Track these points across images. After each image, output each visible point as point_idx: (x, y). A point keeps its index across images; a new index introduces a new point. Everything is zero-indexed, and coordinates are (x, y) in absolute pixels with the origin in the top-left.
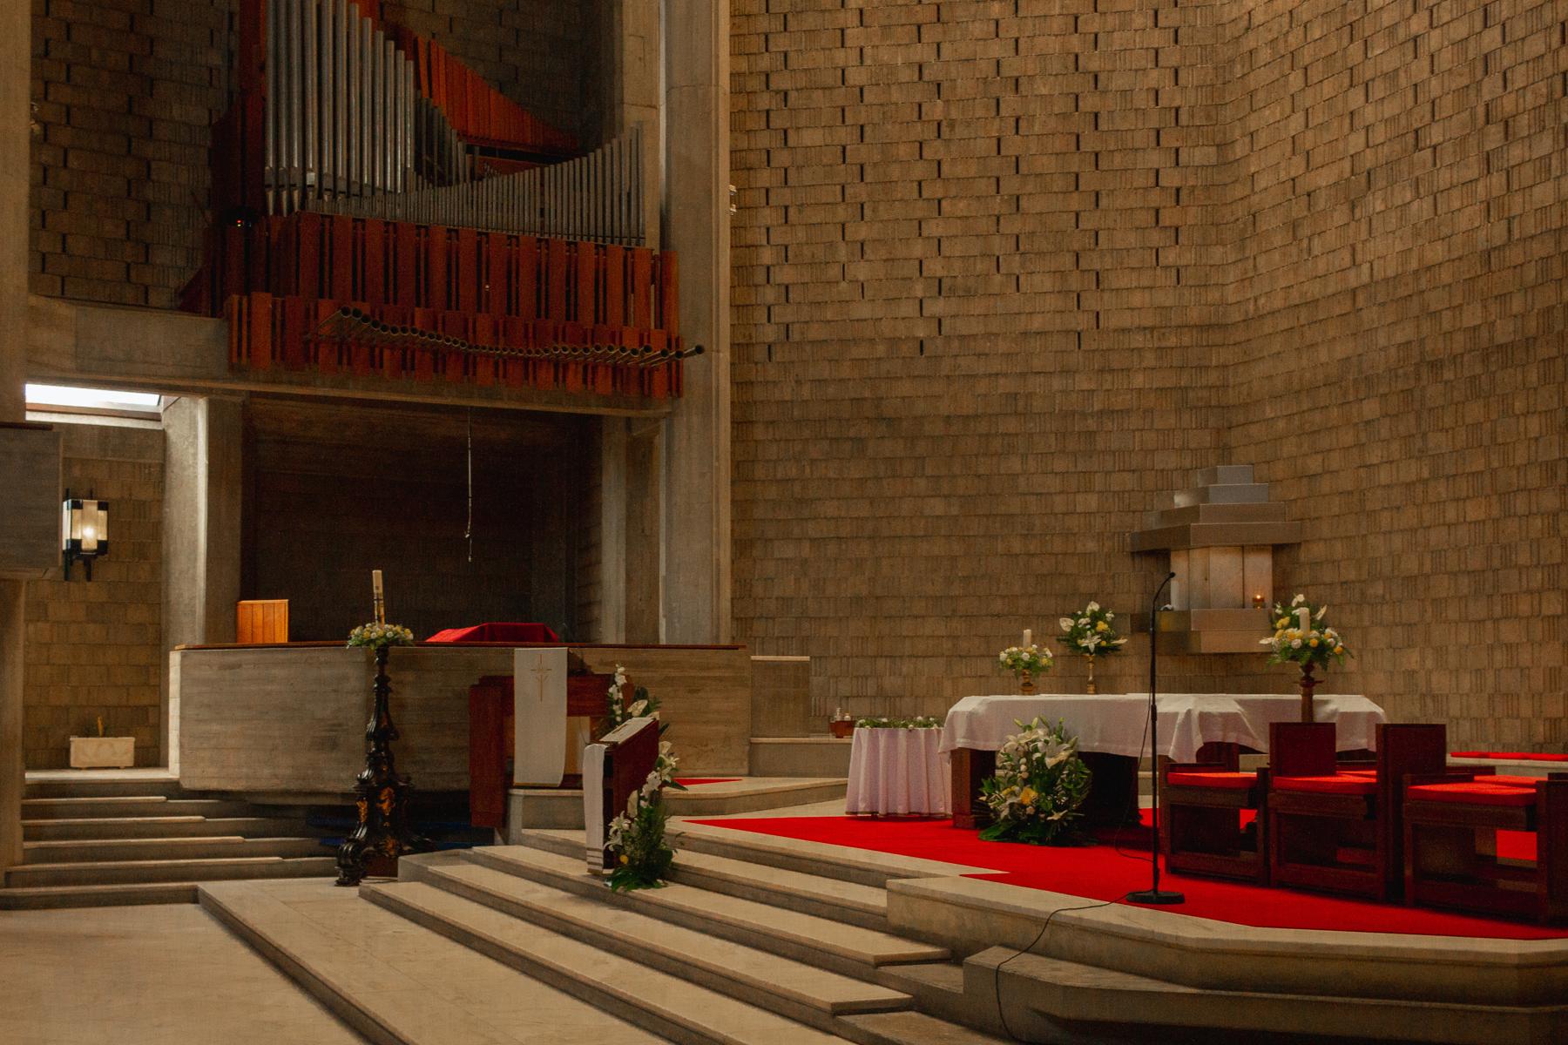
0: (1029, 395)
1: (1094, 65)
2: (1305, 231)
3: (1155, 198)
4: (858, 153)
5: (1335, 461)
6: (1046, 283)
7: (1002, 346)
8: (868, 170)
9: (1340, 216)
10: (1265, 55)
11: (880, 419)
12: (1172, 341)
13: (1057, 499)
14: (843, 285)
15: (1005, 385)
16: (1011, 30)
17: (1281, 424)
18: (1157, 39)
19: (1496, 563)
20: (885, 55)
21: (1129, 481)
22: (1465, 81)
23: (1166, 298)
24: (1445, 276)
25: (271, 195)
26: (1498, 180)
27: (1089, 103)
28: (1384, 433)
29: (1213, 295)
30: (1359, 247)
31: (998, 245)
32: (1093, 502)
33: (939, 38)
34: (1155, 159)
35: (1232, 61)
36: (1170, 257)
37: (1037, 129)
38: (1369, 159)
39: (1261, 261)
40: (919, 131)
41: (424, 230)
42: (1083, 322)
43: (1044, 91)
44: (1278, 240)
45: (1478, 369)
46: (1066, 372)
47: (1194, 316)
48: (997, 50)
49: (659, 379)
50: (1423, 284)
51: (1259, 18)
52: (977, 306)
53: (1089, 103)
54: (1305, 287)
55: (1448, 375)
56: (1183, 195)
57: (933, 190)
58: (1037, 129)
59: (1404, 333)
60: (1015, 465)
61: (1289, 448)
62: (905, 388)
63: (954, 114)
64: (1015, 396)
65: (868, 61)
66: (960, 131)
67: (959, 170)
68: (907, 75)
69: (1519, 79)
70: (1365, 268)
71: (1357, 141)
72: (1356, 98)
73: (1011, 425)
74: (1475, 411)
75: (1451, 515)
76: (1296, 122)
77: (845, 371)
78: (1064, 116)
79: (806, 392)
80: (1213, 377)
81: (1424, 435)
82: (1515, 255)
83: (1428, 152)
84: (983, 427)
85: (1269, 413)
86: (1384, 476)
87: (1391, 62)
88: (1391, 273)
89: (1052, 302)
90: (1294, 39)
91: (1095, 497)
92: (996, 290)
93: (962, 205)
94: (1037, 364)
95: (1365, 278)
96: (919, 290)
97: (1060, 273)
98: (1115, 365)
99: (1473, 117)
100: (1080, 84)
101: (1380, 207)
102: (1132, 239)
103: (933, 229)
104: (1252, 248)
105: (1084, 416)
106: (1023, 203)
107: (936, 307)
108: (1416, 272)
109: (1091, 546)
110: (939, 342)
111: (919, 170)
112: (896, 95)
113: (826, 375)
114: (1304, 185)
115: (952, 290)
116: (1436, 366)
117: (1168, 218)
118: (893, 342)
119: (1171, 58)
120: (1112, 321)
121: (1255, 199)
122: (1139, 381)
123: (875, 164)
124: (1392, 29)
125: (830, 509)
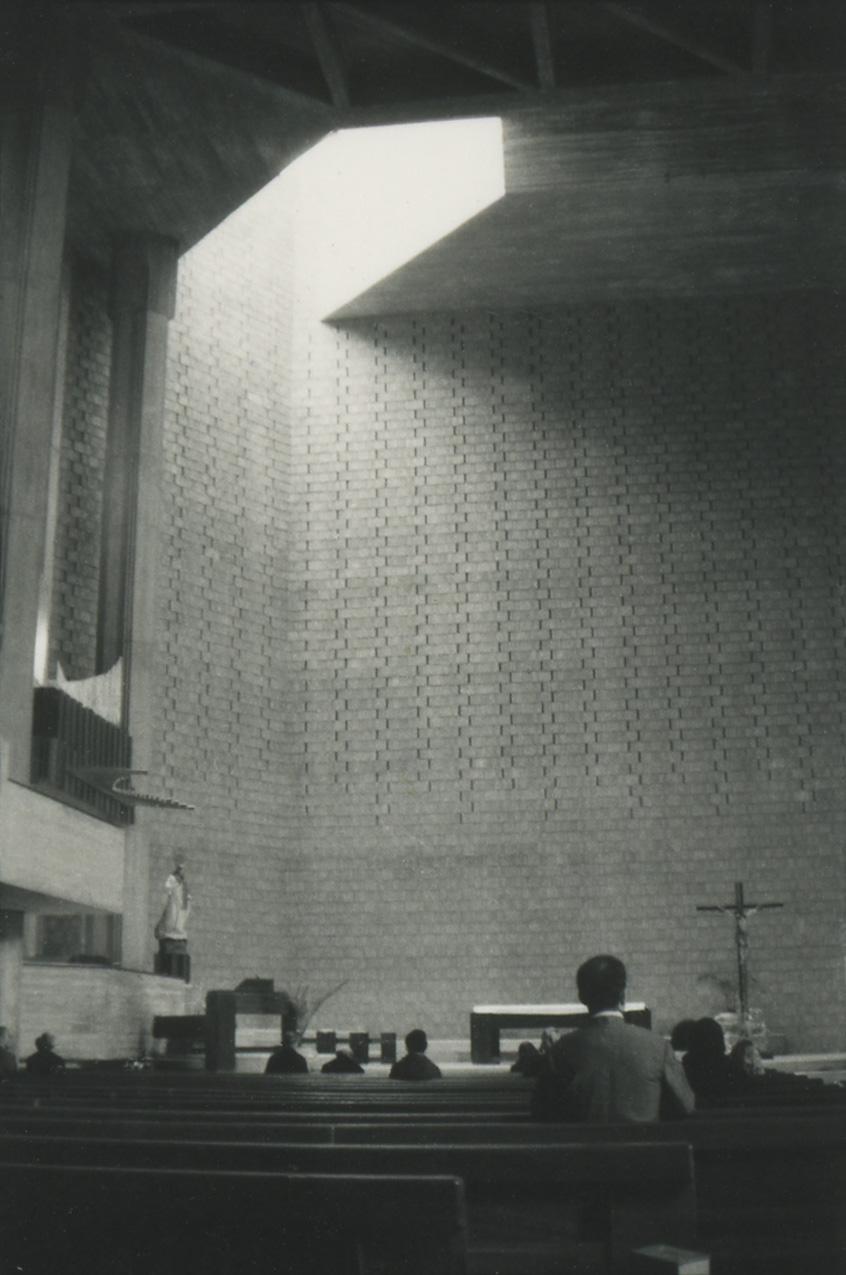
9: (369, 778)
24: (435, 819)
26: (465, 785)
27: (237, 686)
30: (381, 797)
38: (387, 756)
39: (311, 790)
42: (230, 803)
46: (224, 831)
48: (201, 646)
51: (314, 665)
57: (172, 716)
69: (477, 742)
72: (380, 725)
80: (279, 844)
85: (315, 867)
86: (394, 907)
90: (339, 685)
100: (233, 675)
101: (395, 779)
103: (170, 738)
104: (305, 781)
106: (210, 734)
107: (170, 783)
114: (344, 757)
116: (429, 860)
117: (266, 755)
121: (308, 758)
124: (402, 699)
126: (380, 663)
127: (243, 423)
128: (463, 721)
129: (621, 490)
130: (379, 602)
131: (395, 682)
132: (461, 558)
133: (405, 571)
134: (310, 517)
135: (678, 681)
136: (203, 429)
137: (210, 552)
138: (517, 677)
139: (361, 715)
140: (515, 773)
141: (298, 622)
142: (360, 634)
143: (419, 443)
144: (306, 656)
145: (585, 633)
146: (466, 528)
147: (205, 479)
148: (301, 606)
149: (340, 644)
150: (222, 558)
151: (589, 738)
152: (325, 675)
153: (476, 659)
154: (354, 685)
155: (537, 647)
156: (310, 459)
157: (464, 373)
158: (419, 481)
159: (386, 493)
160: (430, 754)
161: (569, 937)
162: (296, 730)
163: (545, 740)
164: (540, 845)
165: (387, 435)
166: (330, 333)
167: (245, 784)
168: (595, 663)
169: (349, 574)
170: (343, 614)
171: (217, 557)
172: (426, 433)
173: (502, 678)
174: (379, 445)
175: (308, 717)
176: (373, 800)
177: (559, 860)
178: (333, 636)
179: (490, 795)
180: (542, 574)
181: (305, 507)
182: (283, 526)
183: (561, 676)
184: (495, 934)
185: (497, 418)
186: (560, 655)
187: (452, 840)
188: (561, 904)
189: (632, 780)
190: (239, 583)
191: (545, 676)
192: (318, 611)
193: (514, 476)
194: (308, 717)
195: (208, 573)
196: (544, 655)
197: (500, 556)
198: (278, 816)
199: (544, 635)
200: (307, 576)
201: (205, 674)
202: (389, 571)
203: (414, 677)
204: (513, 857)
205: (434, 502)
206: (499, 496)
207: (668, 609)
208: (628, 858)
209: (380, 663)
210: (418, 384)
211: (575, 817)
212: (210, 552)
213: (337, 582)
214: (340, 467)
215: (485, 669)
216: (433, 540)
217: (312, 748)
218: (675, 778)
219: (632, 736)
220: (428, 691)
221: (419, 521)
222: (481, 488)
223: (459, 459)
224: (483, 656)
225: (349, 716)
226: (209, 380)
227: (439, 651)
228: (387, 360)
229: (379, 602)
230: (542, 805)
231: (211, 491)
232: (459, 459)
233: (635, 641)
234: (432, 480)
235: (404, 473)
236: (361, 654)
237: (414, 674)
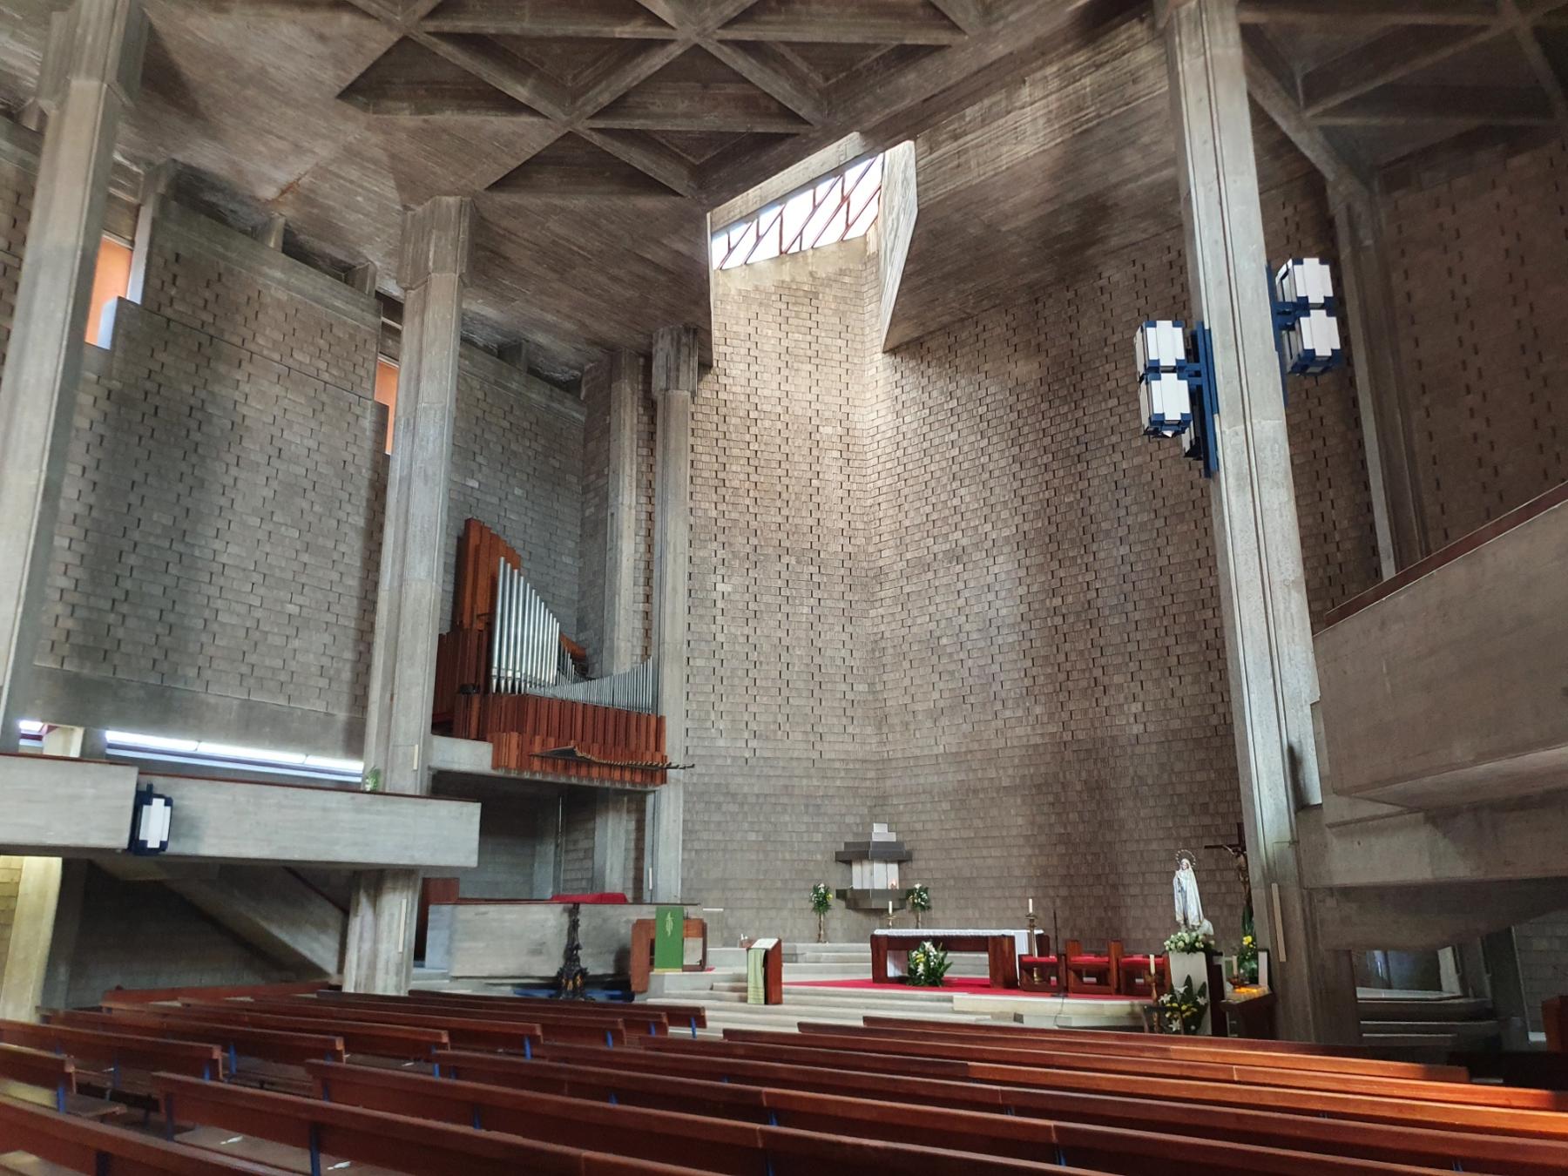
0: (793, 786)
1: (820, 645)
2: (912, 727)
3: (844, 704)
4: (720, 672)
5: (929, 826)
6: (800, 737)
7: (781, 764)
8: (724, 680)
9: (929, 724)
10: (891, 651)
11: (728, 793)
12: (851, 766)
13: (805, 835)
14: (713, 730)
15: (782, 782)
16: (785, 626)
17: (901, 807)
18: (845, 637)
19: (1005, 874)
20: (733, 630)
21: (835, 829)
22: (984, 682)
23: (850, 748)
24: (979, 755)
25: (495, 681)
26: (1000, 723)
27: (817, 660)
28: (953, 816)
29: (868, 748)
31: (780, 718)
32: (818, 837)
33: (756, 625)
34: (844, 687)
36: (850, 730)
37: (796, 669)
38: (941, 704)
39: (890, 736)
40: (747, 665)
41: (573, 703)
42: (815, 755)
43: (798, 653)
44: (898, 729)
45: (995, 795)
46: (809, 777)
47: (860, 756)
49: (658, 774)
50: (969, 757)
51: (887, 635)
52: (770, 745)
53: (817, 660)
54: (913, 750)
55: (981, 796)
56: (855, 703)
58: (796, 669)
59: (962, 776)
60: (787, 818)
61: (906, 818)
62: (740, 780)
63: (762, 659)
64: (786, 787)
65: (725, 631)
66: (765, 667)
67: (764, 683)
68: (742, 640)
69: (1007, 686)
70: (942, 747)
71: (936, 695)
73: (785, 800)
74: (994, 812)
75: (985, 853)
76: (907, 682)
77: (713, 770)
78: (807, 665)
79: (695, 779)
80: (868, 783)
81: (971, 819)
82: (1008, 752)
83: (969, 706)
84: (773, 800)
85: (895, 802)
86: (953, 835)
87: (952, 667)
88: (954, 751)
89: (804, 746)
90: (905, 647)
91: (820, 835)
92: (779, 738)
93: (765, 699)
94: (797, 772)
95: (942, 750)
96: (746, 735)
97: (805, 732)
98: (829, 775)
99: (988, 695)
102: (835, 721)
103: (752, 708)
104: (885, 730)
105: (816, 797)
108: (965, 752)
109: (819, 857)
110: (754, 760)
111: (747, 682)
112: (737, 648)
113: (704, 771)
115: (761, 735)
116: (975, 792)
118: (734, 758)
119: (849, 645)
120: (826, 756)
121: (887, 709)
122: (838, 783)
123: (728, 678)
124: (951, 655)
125: (705, 835)
126: (933, 625)
127: (815, 452)
128: (995, 668)
129: (1115, 439)
131: (944, 641)
132: (988, 527)
133: (948, 547)
135: (1174, 610)
136: (774, 464)
137: (785, 559)
138: (1036, 624)
140: (1038, 710)
143: (954, 436)
144: (883, 628)
145: (1090, 577)
146: (993, 500)
147: (778, 503)
150: (798, 562)
151: (1098, 672)
153: (1004, 612)
154: (915, 647)
155: (1051, 595)
157: (987, 367)
158: (955, 468)
159: (933, 483)
160: (972, 699)
161: (1089, 858)
163: (1062, 677)
164: (1061, 775)
165: (932, 435)
166: (889, 359)
167: (827, 738)
168: (1100, 603)
169: (909, 556)
170: (907, 589)
171: (793, 561)
172: (959, 426)
173: (1024, 627)
174: (926, 445)
175: (885, 677)
176: (933, 742)
177: (1078, 788)
179: (1020, 731)
180: (1053, 529)
181: (877, 507)
182: (860, 526)
183: (1071, 619)
184: (1030, 856)
185: (1013, 399)
186: (1070, 599)
187: (992, 773)
188: (1081, 828)
189: (1136, 708)
190: (815, 578)
191: (1058, 620)
193: (1027, 447)
195: (785, 575)
196: (1057, 601)
197: (1018, 519)
198: (866, 761)
199: (1055, 583)
200: (881, 563)
201: (784, 654)
202: (936, 549)
203: (957, 635)
204: (1038, 787)
205: (967, 483)
206: (1016, 467)
207: (1161, 541)
208: (1137, 783)
209: (933, 625)
210: (952, 387)
211: (1091, 746)
212: (785, 559)
214: (900, 469)
215: (1010, 620)
216: (968, 515)
218: (1174, 703)
219: (1133, 666)
220: (969, 645)
221: (956, 502)
222: (1003, 463)
223: (984, 443)
224: (1007, 610)
225: (912, 673)
226: (779, 425)
227: (976, 609)
229: (930, 575)
230: (1061, 737)
231: (785, 512)
232: (984, 443)
233: (1134, 577)
234: (965, 465)
235: (944, 464)
236: (919, 621)
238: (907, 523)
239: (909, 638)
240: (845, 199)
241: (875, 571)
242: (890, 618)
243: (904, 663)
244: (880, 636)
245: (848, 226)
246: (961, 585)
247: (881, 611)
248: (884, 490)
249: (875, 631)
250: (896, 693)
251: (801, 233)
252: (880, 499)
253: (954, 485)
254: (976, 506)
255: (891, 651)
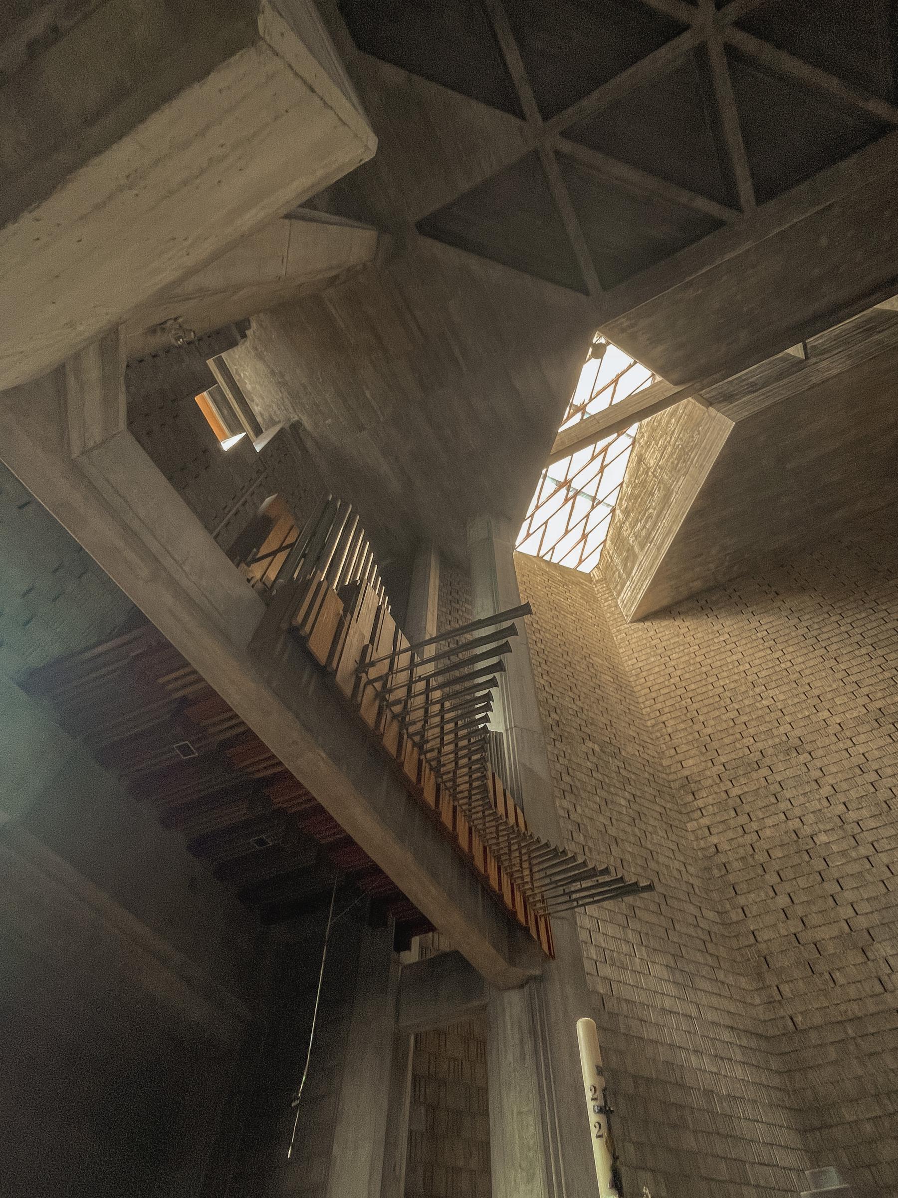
35: (708, 869)
38: (862, 922)
63: (591, 844)
76: (782, 901)
87: (855, 868)
90: (761, 857)
124: (843, 853)
126: (795, 824)
130: (765, 772)
133: (777, 740)
134: (670, 730)
139: (802, 883)
141: (693, 811)
142: (760, 804)
144: (714, 840)
148: (691, 798)
149: (743, 819)
152: (742, 852)
154: (778, 853)
156: (654, 695)
157: (750, 609)
162: (735, 919)
169: (723, 759)
170: (735, 792)
171: (597, 748)
175: (742, 900)
178: (733, 814)
181: (662, 725)
192: (705, 799)
194: (742, 900)
200: (686, 773)
201: (614, 847)
202: (760, 746)
213: (715, 769)
217: (764, 936)
225: (787, 887)
228: (687, 624)
229: (765, 772)
237: (839, 824)
238: (709, 731)
239: (764, 844)
240: (584, 537)
241: (680, 781)
242: (721, 827)
243: (767, 876)
244: (713, 849)
245: (581, 562)
246: (816, 774)
247: (705, 821)
248: (667, 710)
249: (702, 844)
250: (769, 919)
251: (553, 548)
252: (664, 718)
253: (757, 690)
254: (797, 700)
255: (737, 865)
